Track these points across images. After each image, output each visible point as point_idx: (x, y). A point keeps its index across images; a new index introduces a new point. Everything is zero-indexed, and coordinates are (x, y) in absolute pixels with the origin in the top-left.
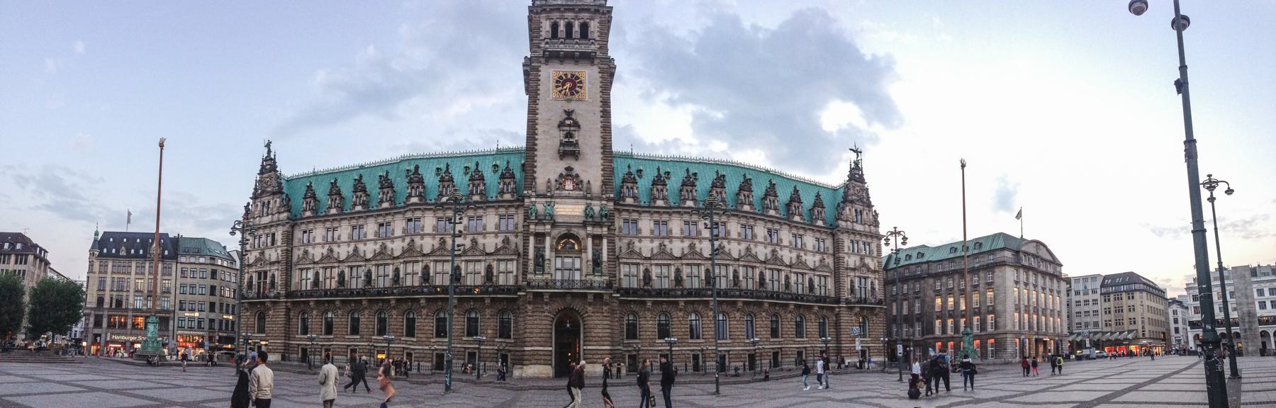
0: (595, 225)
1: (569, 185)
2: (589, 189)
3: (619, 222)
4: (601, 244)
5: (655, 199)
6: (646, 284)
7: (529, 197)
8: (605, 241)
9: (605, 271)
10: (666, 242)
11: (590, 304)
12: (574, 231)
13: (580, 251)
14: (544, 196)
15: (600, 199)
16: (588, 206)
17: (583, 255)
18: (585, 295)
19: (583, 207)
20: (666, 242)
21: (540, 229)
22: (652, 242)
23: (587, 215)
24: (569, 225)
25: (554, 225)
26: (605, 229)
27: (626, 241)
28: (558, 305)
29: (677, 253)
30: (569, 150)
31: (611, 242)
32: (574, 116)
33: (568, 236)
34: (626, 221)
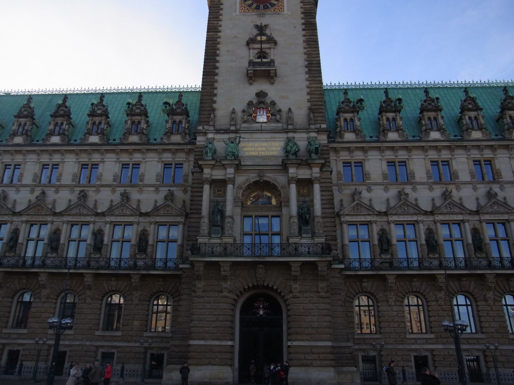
2: (290, 120)
3: (336, 164)
4: (311, 193)
6: (383, 251)
8: (317, 187)
9: (319, 229)
10: (408, 189)
11: (295, 279)
12: (269, 177)
13: (280, 206)
14: (227, 131)
15: (307, 130)
16: (289, 140)
17: (284, 210)
19: (282, 144)
21: (218, 174)
22: (386, 190)
23: (287, 152)
24: (261, 168)
25: (238, 167)
27: (348, 191)
29: (426, 206)
30: (262, 70)
31: (327, 190)
32: (268, 32)
33: (262, 185)
34: (347, 164)
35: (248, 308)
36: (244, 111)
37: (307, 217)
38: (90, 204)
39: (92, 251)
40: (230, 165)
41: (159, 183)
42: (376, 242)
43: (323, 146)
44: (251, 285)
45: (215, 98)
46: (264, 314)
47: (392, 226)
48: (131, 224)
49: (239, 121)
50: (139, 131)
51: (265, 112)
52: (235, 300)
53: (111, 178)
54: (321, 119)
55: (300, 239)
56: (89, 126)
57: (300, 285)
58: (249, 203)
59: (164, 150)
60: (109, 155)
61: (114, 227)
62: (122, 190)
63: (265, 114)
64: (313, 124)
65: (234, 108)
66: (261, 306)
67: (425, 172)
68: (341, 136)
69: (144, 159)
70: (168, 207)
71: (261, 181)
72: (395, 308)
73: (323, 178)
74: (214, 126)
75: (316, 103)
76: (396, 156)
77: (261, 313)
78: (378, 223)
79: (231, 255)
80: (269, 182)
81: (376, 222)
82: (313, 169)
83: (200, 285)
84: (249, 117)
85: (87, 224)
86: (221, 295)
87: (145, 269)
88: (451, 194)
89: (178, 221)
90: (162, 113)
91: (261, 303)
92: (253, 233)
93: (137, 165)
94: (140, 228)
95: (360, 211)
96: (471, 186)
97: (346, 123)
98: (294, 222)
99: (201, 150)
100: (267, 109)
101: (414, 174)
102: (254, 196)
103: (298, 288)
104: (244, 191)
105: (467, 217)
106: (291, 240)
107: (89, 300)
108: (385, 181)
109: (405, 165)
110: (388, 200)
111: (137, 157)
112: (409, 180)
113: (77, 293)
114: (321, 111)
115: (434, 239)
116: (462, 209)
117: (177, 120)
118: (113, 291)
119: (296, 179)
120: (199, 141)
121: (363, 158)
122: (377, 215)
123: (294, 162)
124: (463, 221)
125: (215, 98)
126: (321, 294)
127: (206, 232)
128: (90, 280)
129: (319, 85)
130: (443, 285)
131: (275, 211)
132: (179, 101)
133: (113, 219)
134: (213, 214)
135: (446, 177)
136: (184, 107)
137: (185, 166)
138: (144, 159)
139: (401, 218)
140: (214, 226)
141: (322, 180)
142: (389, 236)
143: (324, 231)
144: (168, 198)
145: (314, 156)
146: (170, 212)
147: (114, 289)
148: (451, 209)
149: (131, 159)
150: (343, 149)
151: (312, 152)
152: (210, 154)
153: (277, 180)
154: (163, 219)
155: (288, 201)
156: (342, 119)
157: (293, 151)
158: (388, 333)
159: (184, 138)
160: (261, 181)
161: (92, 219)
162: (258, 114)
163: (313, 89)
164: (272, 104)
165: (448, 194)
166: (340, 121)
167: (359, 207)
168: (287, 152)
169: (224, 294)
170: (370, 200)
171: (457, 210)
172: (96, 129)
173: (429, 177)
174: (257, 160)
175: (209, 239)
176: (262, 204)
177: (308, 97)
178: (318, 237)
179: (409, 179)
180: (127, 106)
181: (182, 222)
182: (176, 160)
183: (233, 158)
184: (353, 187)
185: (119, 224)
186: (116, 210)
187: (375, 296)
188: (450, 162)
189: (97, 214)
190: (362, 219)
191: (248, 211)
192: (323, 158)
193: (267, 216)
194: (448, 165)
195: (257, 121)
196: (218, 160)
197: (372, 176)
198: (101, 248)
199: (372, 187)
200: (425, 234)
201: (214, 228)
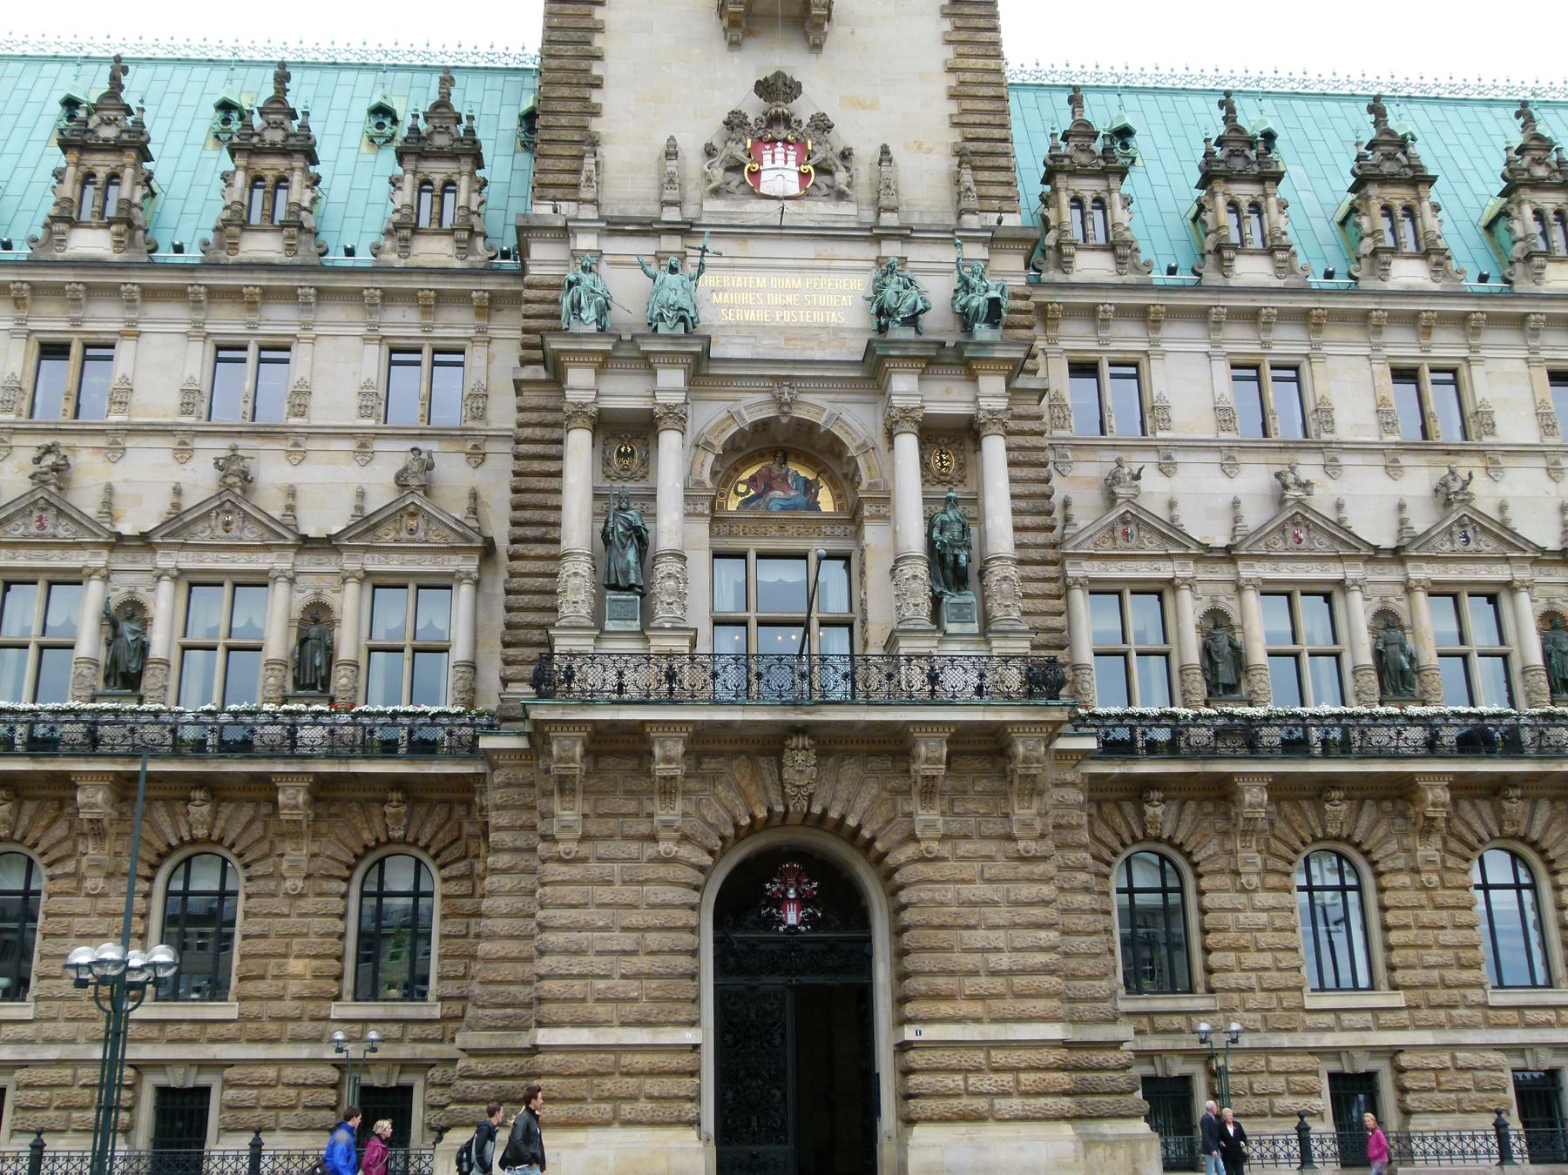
0: (935, 360)
1: (780, 172)
2: (883, 196)
5: (1221, 253)
6: (1219, 689)
7: (564, 233)
8: (995, 449)
9: (1007, 608)
10: (1309, 468)
11: (929, 791)
12: (817, 407)
13: (853, 519)
14: (647, 228)
15: (952, 236)
16: (887, 269)
17: (873, 534)
18: (891, 745)
20: (1309, 468)
21: (624, 393)
22: (1229, 467)
24: (783, 377)
25: (702, 368)
26: (992, 385)
28: (733, 801)
34: (1083, 369)
35: (741, 902)
36: (710, 151)
37: (963, 559)
38: (86, 500)
39: (100, 686)
40: (671, 358)
41: (371, 422)
42: (1193, 656)
43: (1015, 296)
44: (761, 813)
45: (596, 96)
46: (802, 922)
47: (1251, 597)
48: (261, 581)
49: (693, 192)
50: (280, 215)
51: (792, 156)
52: (702, 869)
53: (174, 400)
54: (999, 191)
55: (940, 641)
56: (69, 189)
57: (943, 814)
58: (733, 504)
59: (389, 297)
60: (157, 310)
61: (190, 592)
62: (221, 447)
63: (792, 164)
64: (973, 212)
65: (672, 138)
66: (792, 894)
67: (1372, 406)
68: (1063, 263)
69: (306, 326)
70: (413, 515)
72: (1263, 899)
73: (1014, 417)
74: (594, 202)
75: (981, 132)
76: (1264, 344)
77: (792, 917)
78: (1199, 588)
79: (693, 701)
80: (811, 427)
81: (1191, 584)
82: (982, 379)
83: (567, 813)
84: (731, 176)
85: (75, 579)
86: (650, 850)
87: (330, 756)
88: (1470, 489)
89: (451, 569)
90: (365, 148)
91: (792, 881)
92: (752, 616)
93: (276, 350)
95: (1134, 542)
96: (1541, 462)
97: (1077, 212)
98: (915, 577)
99: (551, 294)
100: (799, 144)
102: (753, 479)
103: (940, 824)
104: (717, 456)
105: (1523, 574)
106: (905, 646)
107: (94, 882)
108: (1224, 435)
109: (1297, 379)
110: (1236, 504)
111: (278, 320)
112: (1312, 433)
113: (43, 854)
114: (1002, 162)
115: (1402, 647)
116: (1510, 544)
117: (438, 180)
118: (194, 841)
119: (919, 415)
120: (542, 263)
121: (1143, 346)
122: (1198, 559)
123: (911, 353)
124: (1509, 586)
125: (596, 96)
126: (1021, 845)
127: (584, 610)
128: (100, 797)
129: (992, 64)
130: (1441, 814)
131: (833, 536)
132: (443, 104)
133: (188, 561)
134: (607, 541)
135: (1447, 429)
136: (461, 129)
137: (475, 357)
138: (306, 326)
139: (1286, 572)
141: (1012, 425)
142: (1238, 637)
143: (1024, 613)
144: (413, 482)
145: (983, 332)
147: (201, 832)
148: (1468, 541)
150: (1071, 311)
151: (976, 318)
152: (589, 314)
153: (845, 417)
154: (394, 564)
155: (885, 499)
156: (1064, 199)
157: (905, 311)
158: (1240, 990)
159: (464, 248)
160: (785, 420)
161: (99, 560)
162: (767, 163)
163: (968, 77)
164: (817, 128)
165: (1456, 486)
166: (1057, 205)
167: (1131, 529)
168: (880, 312)
169: (662, 847)
170: (1172, 505)
171: (1488, 546)
172: (98, 202)
173: (1387, 425)
174: (766, 342)
175: (597, 639)
176: (784, 508)
177: (953, 107)
178: (1004, 634)
179: (1312, 427)
180: (220, 114)
181: (468, 574)
182: (438, 333)
183: (680, 329)
184: (1111, 456)
185: (212, 581)
186: (199, 527)
187: (1188, 855)
188: (1463, 373)
189: (118, 543)
190: (1143, 571)
191: (730, 534)
192: (1019, 342)
193: (803, 556)
194: (1455, 382)
195: (764, 189)
196: (627, 337)
197: (1177, 415)
198: (140, 674)
199: (1178, 457)
200: (1373, 630)
201: (611, 595)
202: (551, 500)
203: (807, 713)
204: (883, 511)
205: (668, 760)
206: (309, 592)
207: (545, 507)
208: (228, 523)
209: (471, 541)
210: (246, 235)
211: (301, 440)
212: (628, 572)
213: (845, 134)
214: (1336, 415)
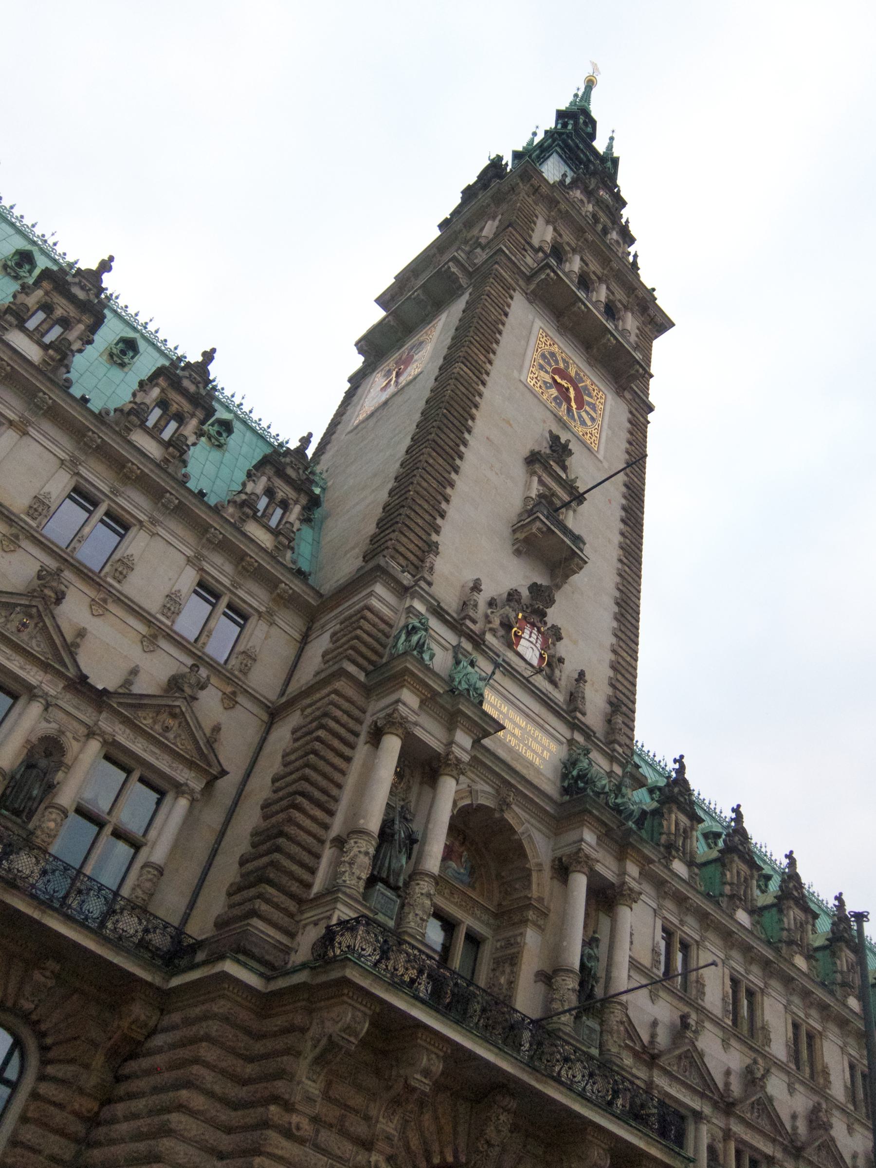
12: (519, 819)
67: (721, 996)
69: (154, 521)
70: (174, 716)
71: (497, 815)
76: (681, 921)
80: (511, 829)
94: (44, 724)
101: (704, 986)
111: (135, 503)
120: (381, 600)
123: (604, 818)
131: (479, 919)
140: (386, 883)
146: (171, 735)
149: (115, 491)
154: (139, 747)
160: (497, 815)
162: (526, 635)
163: (621, 661)
171: (764, 1124)
181: (192, 792)
195: (520, 649)
202: (337, 776)
203: (537, 1080)
204: (541, 922)
205: (426, 1073)
206: (54, 725)
207: (332, 781)
208: (24, 625)
209: (210, 766)
210: (139, 431)
211: (110, 600)
212: (399, 875)
213: (562, 649)
214: (707, 990)
